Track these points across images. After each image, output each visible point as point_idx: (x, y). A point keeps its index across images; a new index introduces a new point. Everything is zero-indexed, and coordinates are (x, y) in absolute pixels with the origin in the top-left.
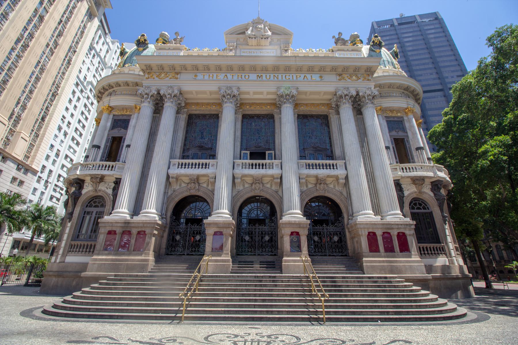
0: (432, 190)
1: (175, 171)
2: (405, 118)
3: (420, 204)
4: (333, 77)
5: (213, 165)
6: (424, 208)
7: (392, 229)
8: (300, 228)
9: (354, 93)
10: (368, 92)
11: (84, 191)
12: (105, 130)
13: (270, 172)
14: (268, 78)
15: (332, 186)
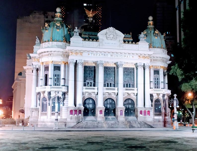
0: (162, 97)
1: (85, 91)
2: (160, 70)
3: (158, 101)
4: (136, 57)
5: (96, 89)
6: (159, 102)
7: (147, 110)
8: (123, 109)
9: (143, 65)
10: (148, 65)
11: (52, 96)
12: (52, 71)
13: (114, 91)
14: (115, 56)
15: (132, 96)
